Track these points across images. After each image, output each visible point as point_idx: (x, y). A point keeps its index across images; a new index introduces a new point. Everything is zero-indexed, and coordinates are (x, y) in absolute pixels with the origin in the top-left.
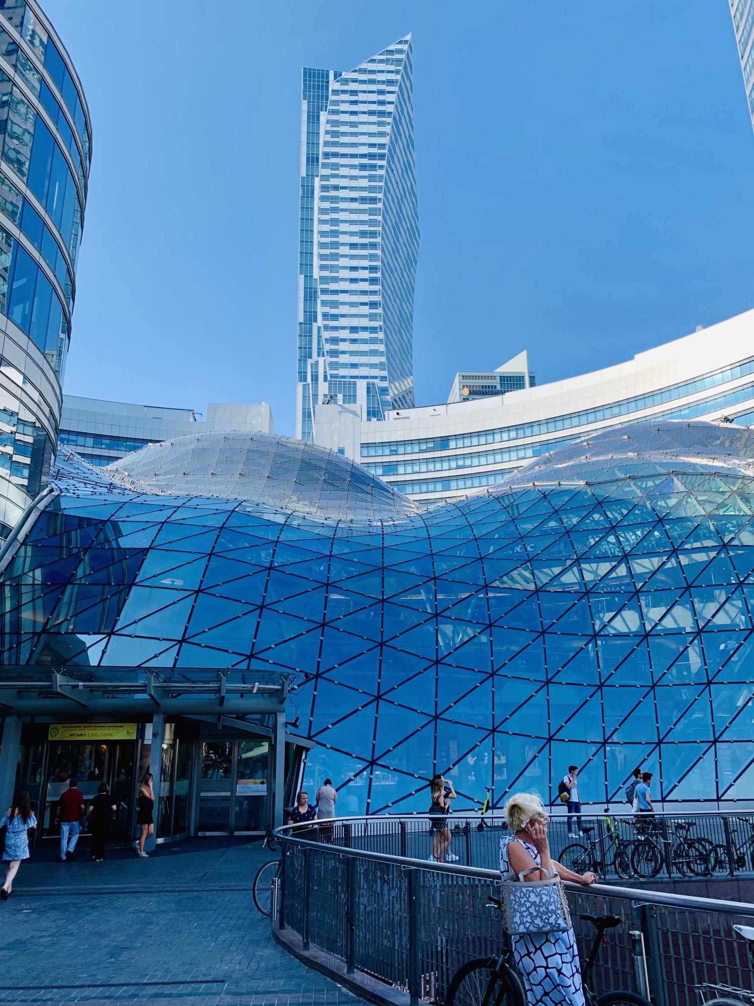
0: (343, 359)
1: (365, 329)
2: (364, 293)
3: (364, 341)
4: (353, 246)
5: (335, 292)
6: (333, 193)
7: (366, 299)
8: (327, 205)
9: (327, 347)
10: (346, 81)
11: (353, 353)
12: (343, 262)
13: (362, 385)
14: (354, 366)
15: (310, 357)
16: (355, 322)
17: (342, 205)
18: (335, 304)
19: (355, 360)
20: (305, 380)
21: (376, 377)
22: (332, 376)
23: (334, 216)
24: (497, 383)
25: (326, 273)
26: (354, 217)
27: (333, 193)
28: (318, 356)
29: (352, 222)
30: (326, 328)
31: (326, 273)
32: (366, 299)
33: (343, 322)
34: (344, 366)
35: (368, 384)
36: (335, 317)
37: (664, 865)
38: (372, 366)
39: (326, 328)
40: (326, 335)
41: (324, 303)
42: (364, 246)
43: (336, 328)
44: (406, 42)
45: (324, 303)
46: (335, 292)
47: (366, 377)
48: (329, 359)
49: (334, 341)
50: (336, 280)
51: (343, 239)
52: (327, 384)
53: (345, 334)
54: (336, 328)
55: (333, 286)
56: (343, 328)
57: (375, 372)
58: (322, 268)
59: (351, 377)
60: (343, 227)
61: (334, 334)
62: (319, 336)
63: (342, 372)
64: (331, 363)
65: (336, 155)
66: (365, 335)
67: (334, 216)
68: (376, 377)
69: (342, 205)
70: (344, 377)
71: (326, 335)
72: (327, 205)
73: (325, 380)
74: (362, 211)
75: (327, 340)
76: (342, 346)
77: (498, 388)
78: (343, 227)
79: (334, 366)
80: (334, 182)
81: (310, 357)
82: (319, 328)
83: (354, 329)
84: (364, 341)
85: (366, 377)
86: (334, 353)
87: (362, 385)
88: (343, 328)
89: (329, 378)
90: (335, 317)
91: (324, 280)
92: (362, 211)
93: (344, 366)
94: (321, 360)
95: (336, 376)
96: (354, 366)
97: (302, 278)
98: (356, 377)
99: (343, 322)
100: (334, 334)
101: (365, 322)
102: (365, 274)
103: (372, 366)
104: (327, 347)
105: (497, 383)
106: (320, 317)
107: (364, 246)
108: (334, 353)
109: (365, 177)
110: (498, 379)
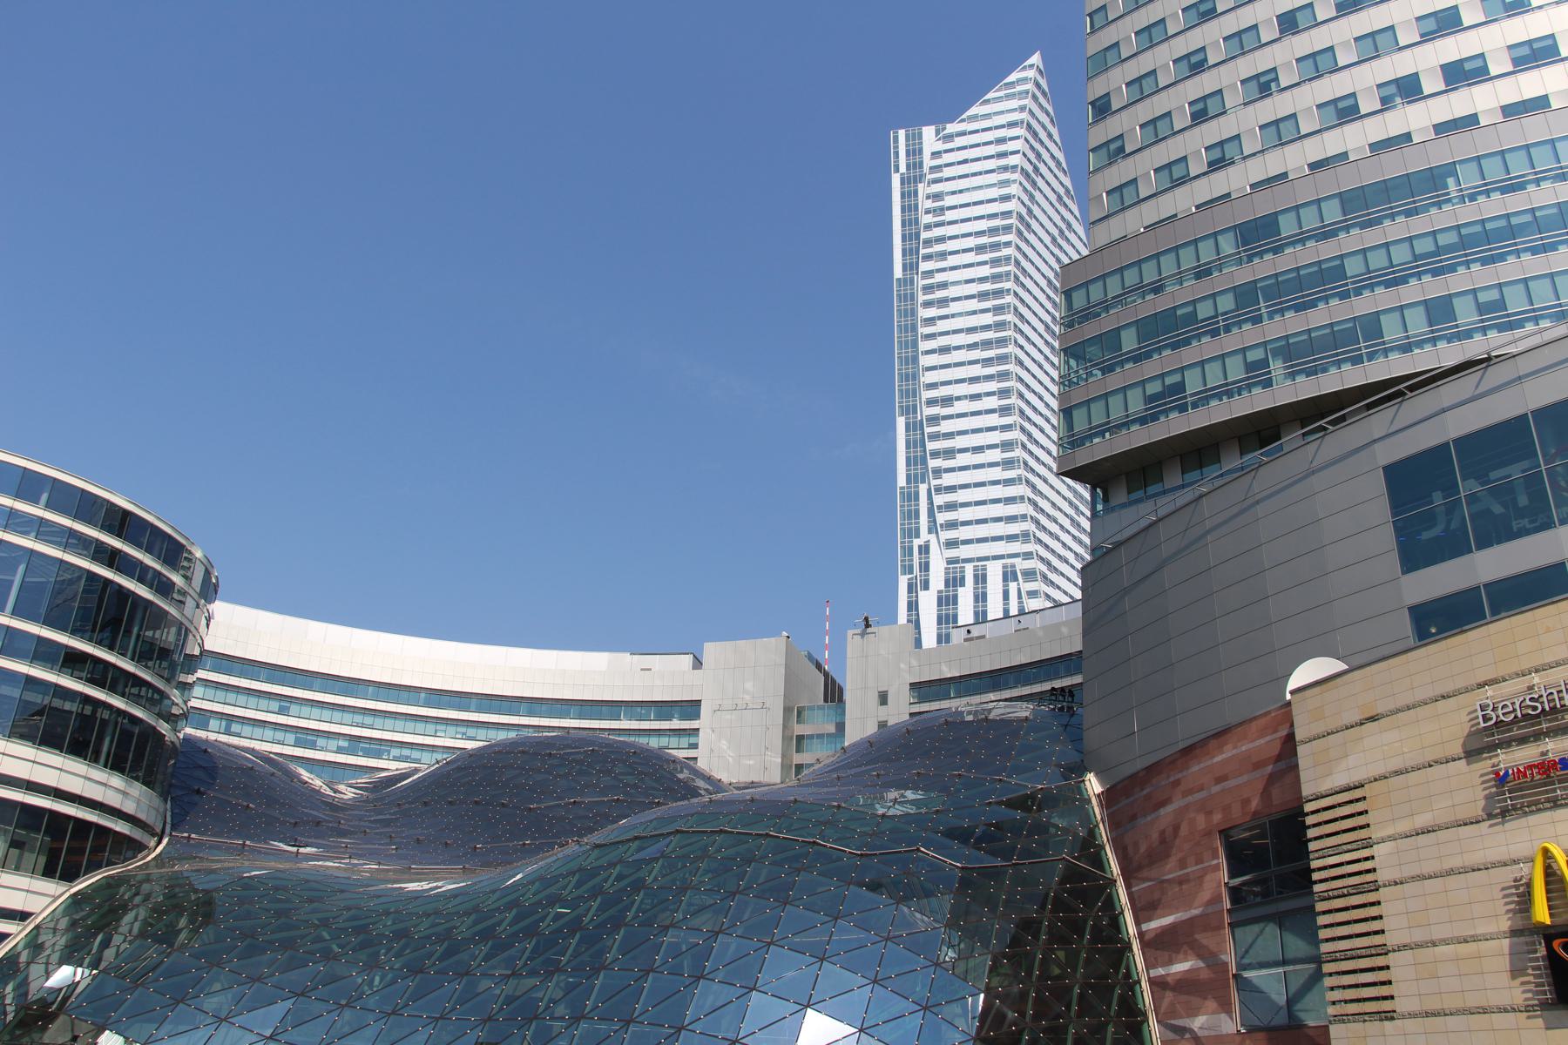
5: (949, 435)
6: (940, 294)
10: (949, 138)
13: (994, 571)
15: (918, 536)
21: (1016, 555)
27: (940, 294)
28: (930, 532)
30: (939, 490)
39: (939, 490)
40: (939, 500)
41: (935, 454)
44: (1032, 66)
45: (935, 454)
46: (949, 435)
47: (1001, 557)
62: (931, 503)
65: (941, 240)
68: (1016, 555)
71: (939, 500)
72: (932, 312)
75: (940, 507)
80: (939, 278)
81: (918, 536)
82: (929, 491)
85: (1001, 557)
87: (994, 571)
91: (934, 420)
94: (932, 538)
97: (901, 422)
98: (986, 559)
102: (993, 402)
104: (941, 518)
109: (985, 263)
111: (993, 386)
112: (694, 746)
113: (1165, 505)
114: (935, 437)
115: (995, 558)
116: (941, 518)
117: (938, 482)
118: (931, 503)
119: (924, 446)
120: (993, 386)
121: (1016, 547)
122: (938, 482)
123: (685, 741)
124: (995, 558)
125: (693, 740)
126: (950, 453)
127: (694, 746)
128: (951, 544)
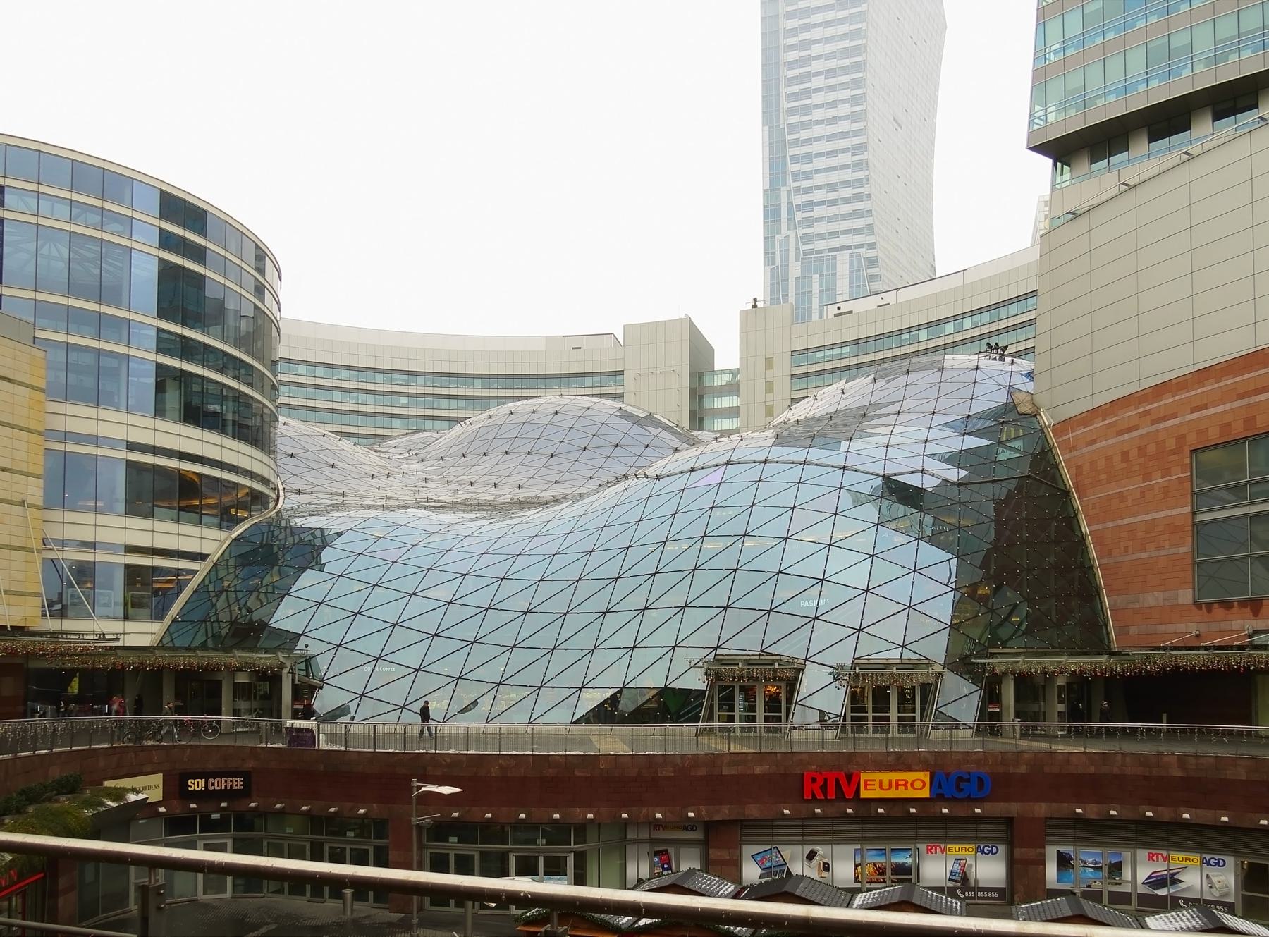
0: (820, 228)
1: (846, 184)
2: (845, 135)
3: (847, 200)
4: (830, 73)
5: (808, 142)
7: (846, 143)
8: (794, 23)
9: (799, 215)
11: (832, 219)
12: (817, 99)
13: (843, 257)
14: (834, 234)
16: (833, 177)
17: (815, 18)
18: (808, 158)
19: (834, 227)
21: (861, 246)
22: (806, 253)
23: (803, 36)
25: (795, 119)
26: (830, 32)
29: (828, 40)
30: (798, 191)
31: (795, 119)
32: (846, 143)
33: (819, 179)
34: (821, 237)
35: (851, 256)
36: (808, 175)
39: (798, 191)
41: (795, 159)
42: (844, 70)
43: (808, 190)
45: (795, 159)
46: (808, 142)
47: (850, 248)
48: (801, 231)
49: (808, 206)
50: (807, 125)
51: (817, 66)
53: (820, 195)
54: (808, 190)
55: (805, 134)
56: (819, 187)
58: (791, 112)
59: (830, 250)
60: (817, 50)
61: (807, 197)
62: (790, 203)
63: (819, 245)
64: (804, 237)
66: (846, 192)
67: (803, 36)
68: (861, 246)
69: (815, 18)
70: (820, 252)
71: (797, 200)
72: (794, 23)
74: (841, 21)
75: (798, 206)
76: (819, 211)
78: (817, 50)
79: (809, 238)
81: (779, 232)
82: (789, 192)
83: (832, 187)
84: (847, 200)
85: (850, 248)
87: (843, 257)
88: (819, 187)
90: (808, 175)
91: (794, 128)
92: (841, 21)
93: (821, 237)
94: (792, 234)
95: (810, 252)
96: (834, 234)
98: (836, 249)
99: (819, 179)
100: (807, 197)
101: (846, 175)
106: (789, 178)
107: (844, 70)
108: (809, 222)
111: (846, 94)
113: (1132, 174)
114: (795, 143)
115: (844, 248)
116: (799, 215)
117: (797, 184)
118: (790, 203)
119: (785, 151)
120: (846, 94)
121: (860, 239)
122: (797, 184)
124: (844, 248)
126: (808, 158)
128: (809, 238)
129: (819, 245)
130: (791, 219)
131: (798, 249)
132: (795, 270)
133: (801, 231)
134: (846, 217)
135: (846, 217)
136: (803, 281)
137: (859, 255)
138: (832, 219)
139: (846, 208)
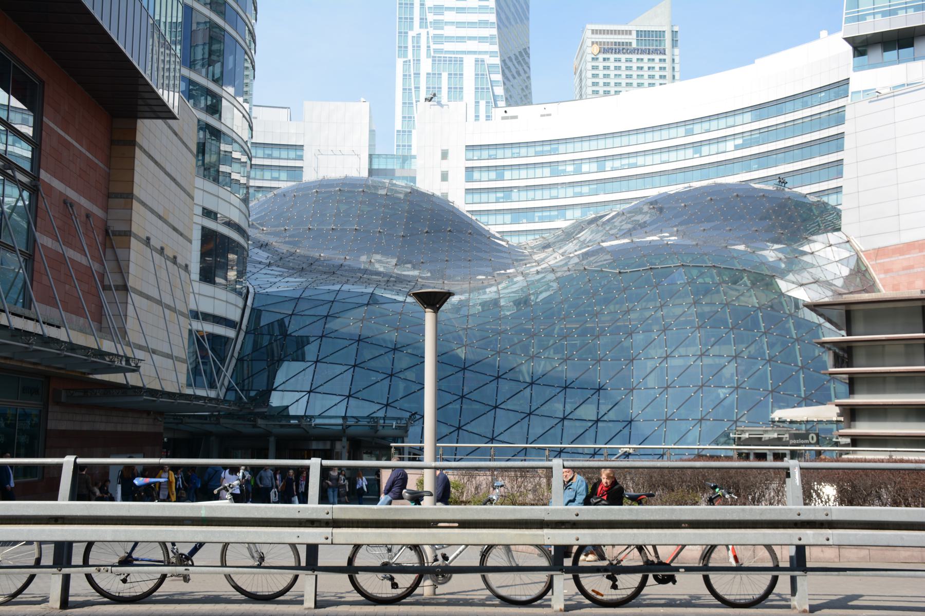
0: (449, 31)
11: (459, 25)
14: (461, 39)
20: (405, 56)
22: (435, 51)
24: (632, 39)
34: (450, 39)
35: (477, 61)
37: (850, 603)
38: (482, 39)
48: (432, 32)
52: (430, 60)
57: (486, 47)
63: (448, 46)
64: (435, 36)
68: (485, 53)
73: (428, 56)
76: (449, 16)
77: (634, 45)
79: (438, 39)
81: (411, 29)
85: (475, 53)
86: (437, 24)
89: (432, 54)
93: (450, 39)
94: (423, 32)
95: (441, 51)
96: (461, 39)
103: (482, 39)
105: (632, 39)
110: (634, 34)
112: (300, 158)
116: (431, 17)
123: (292, 154)
125: (299, 153)
127: (300, 158)
128: (438, 39)
129: (448, 46)
130: (423, 20)
131: (429, 47)
132: (426, 66)
133: (432, 32)
134: (472, 25)
135: (472, 25)
136: (434, 76)
137: (483, 61)
138: (459, 25)
139: (474, 18)
